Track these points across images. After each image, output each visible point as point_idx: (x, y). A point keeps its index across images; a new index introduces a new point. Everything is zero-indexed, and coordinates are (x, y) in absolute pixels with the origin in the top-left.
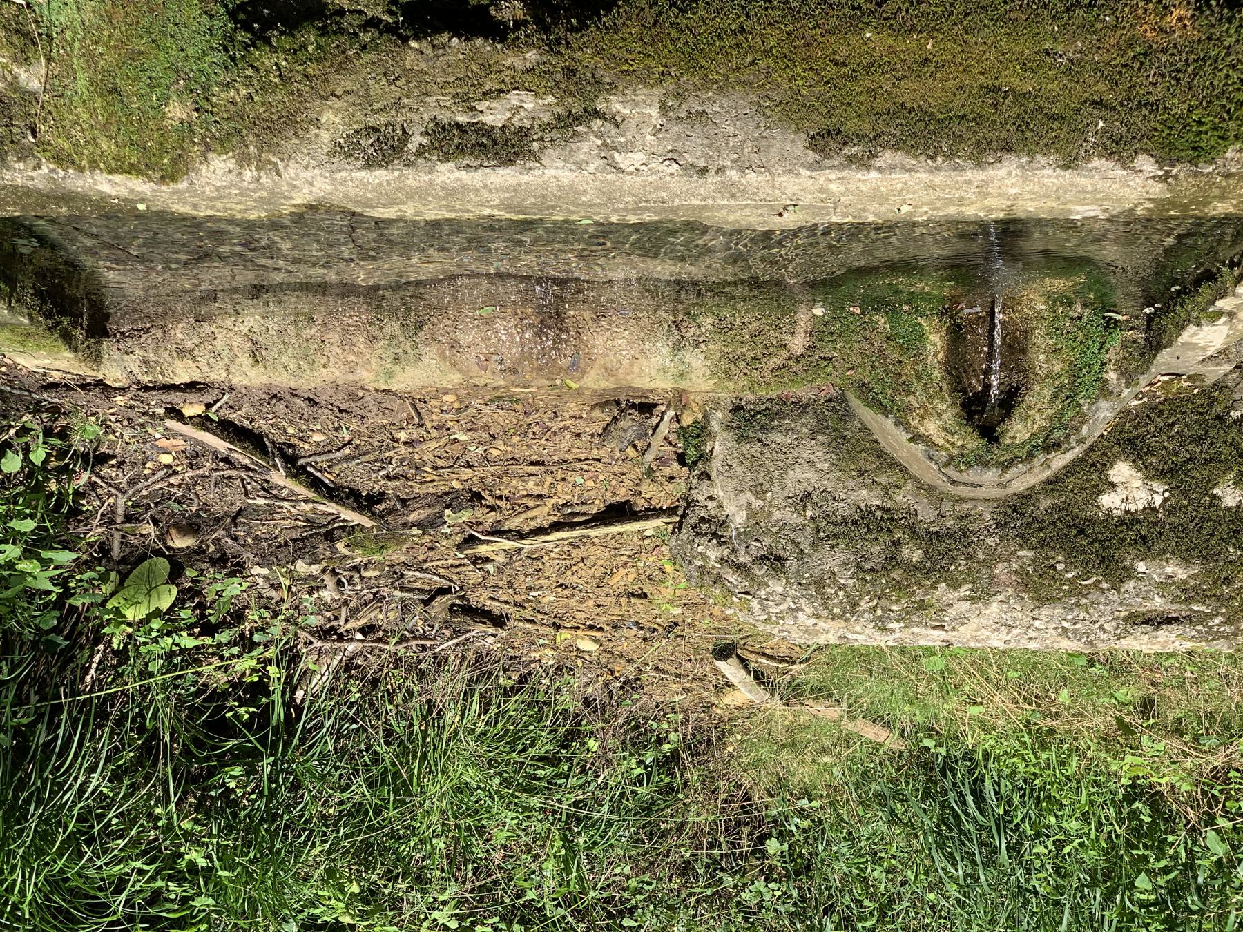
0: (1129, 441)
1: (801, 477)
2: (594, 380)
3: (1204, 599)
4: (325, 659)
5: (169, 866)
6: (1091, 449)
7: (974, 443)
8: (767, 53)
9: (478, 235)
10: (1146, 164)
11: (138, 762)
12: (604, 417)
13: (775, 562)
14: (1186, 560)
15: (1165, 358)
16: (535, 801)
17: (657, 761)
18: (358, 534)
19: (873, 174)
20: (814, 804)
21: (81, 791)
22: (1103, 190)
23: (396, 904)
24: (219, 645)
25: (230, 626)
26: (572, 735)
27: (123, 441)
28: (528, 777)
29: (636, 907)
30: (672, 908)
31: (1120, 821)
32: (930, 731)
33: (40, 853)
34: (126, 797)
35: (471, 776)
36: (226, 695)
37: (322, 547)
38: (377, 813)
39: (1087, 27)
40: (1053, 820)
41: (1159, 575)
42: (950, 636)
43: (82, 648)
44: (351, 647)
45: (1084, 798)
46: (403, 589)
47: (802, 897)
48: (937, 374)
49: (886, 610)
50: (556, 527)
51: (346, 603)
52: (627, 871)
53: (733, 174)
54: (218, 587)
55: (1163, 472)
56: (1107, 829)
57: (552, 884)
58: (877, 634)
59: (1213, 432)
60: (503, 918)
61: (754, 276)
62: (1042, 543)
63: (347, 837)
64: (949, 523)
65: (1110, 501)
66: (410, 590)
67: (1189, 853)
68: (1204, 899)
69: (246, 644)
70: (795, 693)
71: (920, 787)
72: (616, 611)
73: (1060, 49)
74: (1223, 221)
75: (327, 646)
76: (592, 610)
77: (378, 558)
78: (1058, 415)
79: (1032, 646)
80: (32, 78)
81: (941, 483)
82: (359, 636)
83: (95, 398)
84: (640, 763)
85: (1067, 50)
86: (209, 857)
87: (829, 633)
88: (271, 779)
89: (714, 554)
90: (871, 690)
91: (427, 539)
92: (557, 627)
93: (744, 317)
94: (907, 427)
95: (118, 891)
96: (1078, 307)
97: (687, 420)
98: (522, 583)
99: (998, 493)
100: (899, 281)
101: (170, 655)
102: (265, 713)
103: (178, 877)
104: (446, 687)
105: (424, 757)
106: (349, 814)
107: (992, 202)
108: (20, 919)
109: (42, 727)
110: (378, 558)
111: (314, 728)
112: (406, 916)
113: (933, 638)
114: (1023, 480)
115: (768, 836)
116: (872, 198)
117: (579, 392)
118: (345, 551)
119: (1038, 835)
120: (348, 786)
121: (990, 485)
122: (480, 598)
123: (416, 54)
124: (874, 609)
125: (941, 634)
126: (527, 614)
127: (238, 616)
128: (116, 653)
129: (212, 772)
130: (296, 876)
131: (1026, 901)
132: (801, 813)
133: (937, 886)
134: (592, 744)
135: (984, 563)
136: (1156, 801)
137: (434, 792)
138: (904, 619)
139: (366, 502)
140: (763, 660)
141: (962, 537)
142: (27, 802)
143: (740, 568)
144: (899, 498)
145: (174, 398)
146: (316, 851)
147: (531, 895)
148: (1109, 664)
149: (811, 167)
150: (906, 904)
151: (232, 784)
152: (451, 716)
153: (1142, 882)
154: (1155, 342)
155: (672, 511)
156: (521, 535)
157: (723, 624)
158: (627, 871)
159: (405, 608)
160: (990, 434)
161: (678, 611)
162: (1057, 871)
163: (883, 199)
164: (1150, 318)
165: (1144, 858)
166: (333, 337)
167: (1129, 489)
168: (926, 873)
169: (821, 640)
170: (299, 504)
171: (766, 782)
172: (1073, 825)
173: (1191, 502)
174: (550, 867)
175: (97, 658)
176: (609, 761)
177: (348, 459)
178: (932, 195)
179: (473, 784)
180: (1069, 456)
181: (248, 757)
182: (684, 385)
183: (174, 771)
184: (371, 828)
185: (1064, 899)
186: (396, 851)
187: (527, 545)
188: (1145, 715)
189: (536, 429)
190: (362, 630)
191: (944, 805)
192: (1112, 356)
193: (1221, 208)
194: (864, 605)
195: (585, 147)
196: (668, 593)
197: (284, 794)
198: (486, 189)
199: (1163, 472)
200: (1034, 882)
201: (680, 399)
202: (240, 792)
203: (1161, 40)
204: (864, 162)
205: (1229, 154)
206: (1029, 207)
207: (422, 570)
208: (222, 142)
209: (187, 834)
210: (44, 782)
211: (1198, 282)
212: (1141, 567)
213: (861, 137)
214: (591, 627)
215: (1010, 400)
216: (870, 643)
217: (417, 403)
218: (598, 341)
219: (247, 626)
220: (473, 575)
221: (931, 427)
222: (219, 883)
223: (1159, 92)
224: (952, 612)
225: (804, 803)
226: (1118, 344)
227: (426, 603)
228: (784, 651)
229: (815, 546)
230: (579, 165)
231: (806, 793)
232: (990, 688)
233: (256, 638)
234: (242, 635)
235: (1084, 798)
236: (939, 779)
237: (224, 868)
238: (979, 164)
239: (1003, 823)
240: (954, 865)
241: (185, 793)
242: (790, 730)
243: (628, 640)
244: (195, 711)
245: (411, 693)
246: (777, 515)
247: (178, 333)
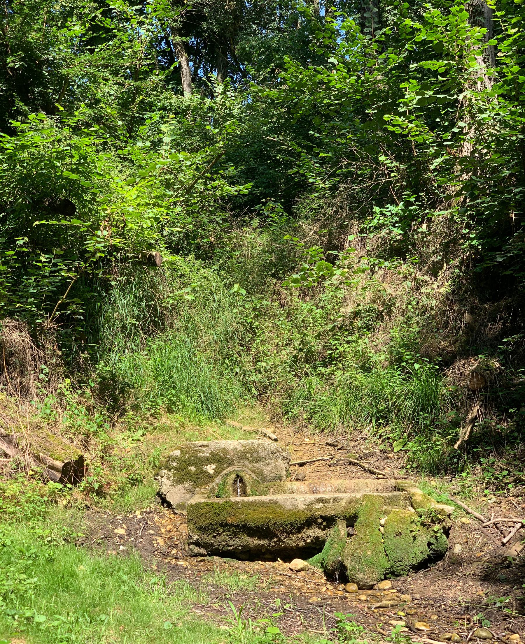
1: (269, 468)
2: (307, 483)
13: (273, 453)
14: (200, 457)
26: (310, 419)
37: (362, 455)
41: (205, 454)
50: (314, 461)
65: (214, 466)
89: (284, 454)
98: (322, 451)
122: (331, 448)
134: (305, 417)
138: (248, 445)
139: (351, 463)
143: (279, 452)
167: (210, 469)
187: (320, 458)
220: (332, 453)
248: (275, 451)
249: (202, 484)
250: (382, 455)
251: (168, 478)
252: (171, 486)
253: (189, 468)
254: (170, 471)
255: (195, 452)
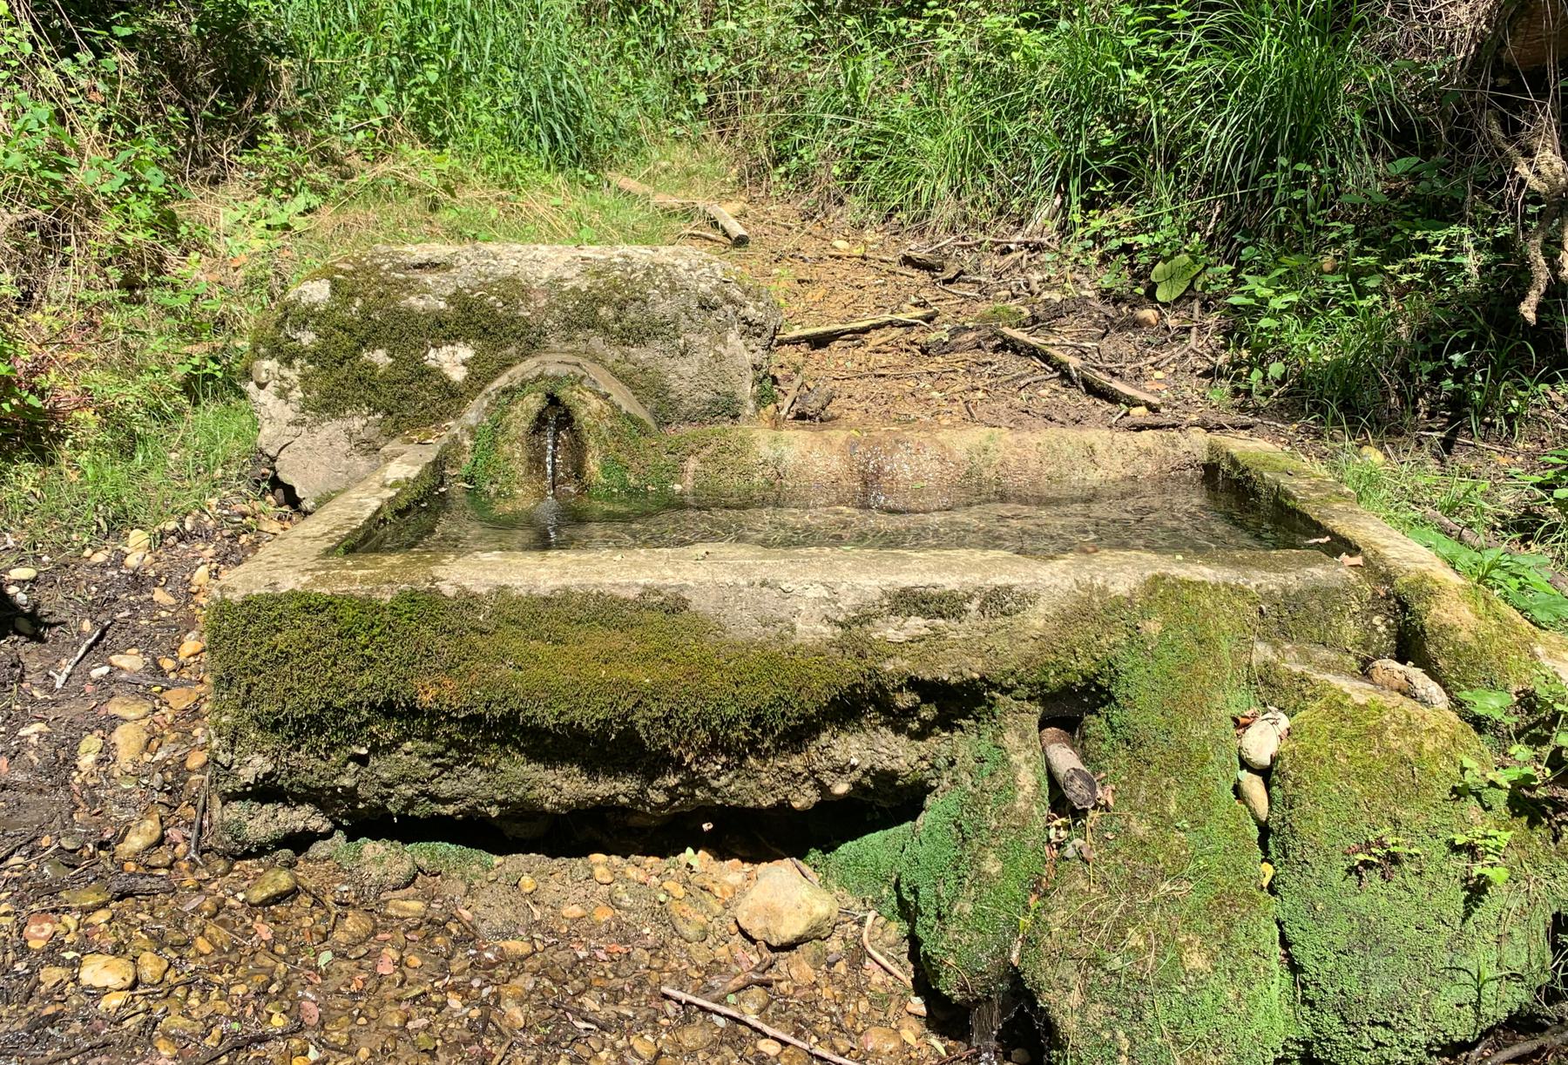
0: (454, 396)
1: (688, 366)
2: (839, 436)
3: (396, 283)
4: (1039, 228)
5: (1157, 70)
6: (480, 390)
7: (563, 393)
8: (719, 668)
9: (919, 539)
10: (448, 590)
11: (1179, 148)
12: (831, 410)
13: (706, 306)
14: (410, 310)
15: (431, 455)
16: (879, 126)
17: (789, 160)
18: (1014, 322)
19: (641, 582)
20: (671, 131)
21: (1224, 123)
22: (477, 571)
23: (984, 45)
24: (1118, 237)
25: (1110, 252)
26: (852, 177)
27: (1192, 388)
28: (884, 144)
29: (804, 48)
30: (776, 48)
31: (450, 122)
32: (589, 186)
33: (1256, 75)
34: (1188, 121)
35: (928, 143)
36: (1114, 200)
37: (1041, 312)
38: (998, 113)
39: (493, 687)
40: (499, 122)
41: (429, 299)
42: (577, 253)
43: (1223, 233)
44: (1019, 238)
45: (477, 138)
46: (979, 283)
47: (680, 60)
48: (592, 443)
49: (624, 271)
50: (866, 330)
51: (1022, 271)
52: (810, 76)
53: (742, 582)
54: (1119, 281)
55: (429, 373)
56: (460, 116)
57: (865, 64)
58: (630, 253)
59: (394, 403)
60: (903, 37)
61: (722, 511)
62: (513, 321)
63: (1022, 95)
64: (580, 335)
65: (465, 352)
66: (973, 282)
67: (399, 98)
68: (388, 65)
69: (1098, 238)
70: (688, 213)
71: (595, 145)
72: (820, 271)
73: (511, 671)
74: (392, 550)
75: (1037, 239)
76: (838, 267)
77: (998, 305)
78: (504, 414)
79: (518, 247)
80: (1262, 652)
81: (587, 365)
82: (1012, 246)
83: (1212, 419)
84: (801, 158)
85: (505, 671)
86: (1126, 77)
87: (664, 254)
88: (1079, 137)
90: (632, 216)
91: (961, 319)
92: (864, 258)
93: (732, 483)
94: (612, 404)
95: (1195, 49)
96: (493, 492)
97: (771, 408)
99: (547, 358)
100: (622, 509)
101: (1155, 229)
102: (1085, 185)
103: (1151, 60)
104: (947, 210)
105: (963, 157)
106: (1020, 112)
107: (556, 562)
108: (1272, 24)
109: (1253, 173)
110: (998, 305)
111: (1047, 176)
112: (976, 36)
113: (590, 251)
114: (528, 367)
115: (705, 106)
116: (642, 565)
117: (850, 427)
118: (1023, 309)
119: (509, 110)
120: (1021, 133)
121: (551, 363)
122: (921, 277)
123: (974, 668)
124: (633, 272)
125: (583, 254)
126: (886, 267)
127: (1104, 259)
128: (1197, 229)
129: (1124, 141)
130: (1059, 64)
131: (517, 61)
132: (681, 122)
133: (583, 71)
134: (836, 171)
135: (555, 306)
136: (425, 136)
137: (956, 129)
138: (610, 266)
140: (712, 236)
141: (571, 325)
142: (1265, 115)
143: (733, 302)
144: (617, 353)
145: (1152, 419)
146: (1046, 83)
147: (883, 55)
148: (462, 237)
149: (687, 586)
150: (604, 58)
151: (1108, 132)
152: (942, 187)
153: (433, 77)
154: (438, 465)
155: (781, 343)
156: (891, 323)
157: (741, 261)
158: (810, 76)
159: (977, 268)
160: (553, 400)
161: (775, 271)
162: (495, 84)
163: (634, 565)
164: (442, 483)
165: (432, 94)
166: (1033, 465)
167: (452, 361)
168: (590, 81)
169: (671, 249)
170: (1060, 343)
171: (707, 146)
172: (485, 118)
173: (408, 352)
174: (868, 76)
175: (1211, 225)
176: (825, 158)
177: (1022, 377)
178: (599, 567)
179: (925, 137)
180: (496, 384)
181: (1097, 153)
182: (774, 433)
183: (1152, 141)
184: (1003, 101)
185: (489, 63)
186: (984, 85)
187: (886, 317)
188: (436, 200)
189: (882, 401)
190: (1010, 251)
191: (578, 131)
192: (468, 457)
193: (394, 559)
194: (640, 274)
195: (849, 601)
196: (783, 284)
197: (1069, 125)
198: (921, 571)
199: (429, 373)
200: (511, 75)
201: (776, 423)
202: (1103, 126)
203: (439, 677)
204: (649, 590)
205: (389, 597)
206: (532, 559)
207: (965, 296)
208: (1119, 604)
209: (1143, 93)
210: (1252, 130)
211: (409, 509)
212: (442, 305)
213: (650, 608)
214: (838, 258)
215: (540, 422)
216: (635, 247)
217: (970, 418)
218: (836, 464)
219: (1098, 252)
220: (926, 294)
221: (595, 404)
222: (1118, 55)
223: (439, 641)
224: (576, 270)
225: (680, 131)
226: (464, 465)
227: (962, 273)
228: (697, 243)
229: (677, 317)
230: (854, 588)
231: (678, 139)
232: (547, 218)
233: (1091, 243)
234: (1101, 245)
235: (477, 138)
236: (577, 145)
237: (1114, 68)
238: (566, 589)
239: (535, 118)
240: (569, 87)
241: (1145, 124)
242: (691, 185)
243: (811, 249)
244: (1137, 187)
245: (973, 204)
246: (705, 340)
247: (1150, 468)
248: (717, 298)
249: (418, 423)
250: (1110, 310)
251: (282, 394)
252: (294, 423)
253: (366, 355)
254: (288, 362)
255: (392, 288)
